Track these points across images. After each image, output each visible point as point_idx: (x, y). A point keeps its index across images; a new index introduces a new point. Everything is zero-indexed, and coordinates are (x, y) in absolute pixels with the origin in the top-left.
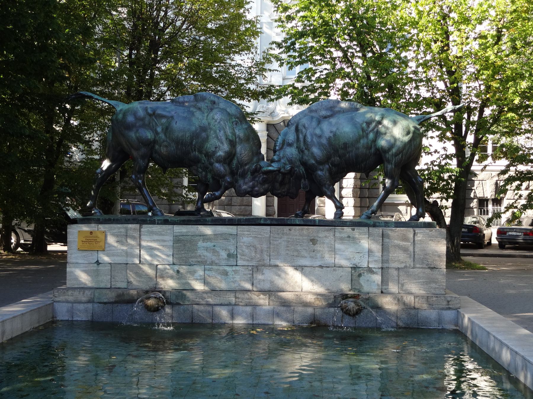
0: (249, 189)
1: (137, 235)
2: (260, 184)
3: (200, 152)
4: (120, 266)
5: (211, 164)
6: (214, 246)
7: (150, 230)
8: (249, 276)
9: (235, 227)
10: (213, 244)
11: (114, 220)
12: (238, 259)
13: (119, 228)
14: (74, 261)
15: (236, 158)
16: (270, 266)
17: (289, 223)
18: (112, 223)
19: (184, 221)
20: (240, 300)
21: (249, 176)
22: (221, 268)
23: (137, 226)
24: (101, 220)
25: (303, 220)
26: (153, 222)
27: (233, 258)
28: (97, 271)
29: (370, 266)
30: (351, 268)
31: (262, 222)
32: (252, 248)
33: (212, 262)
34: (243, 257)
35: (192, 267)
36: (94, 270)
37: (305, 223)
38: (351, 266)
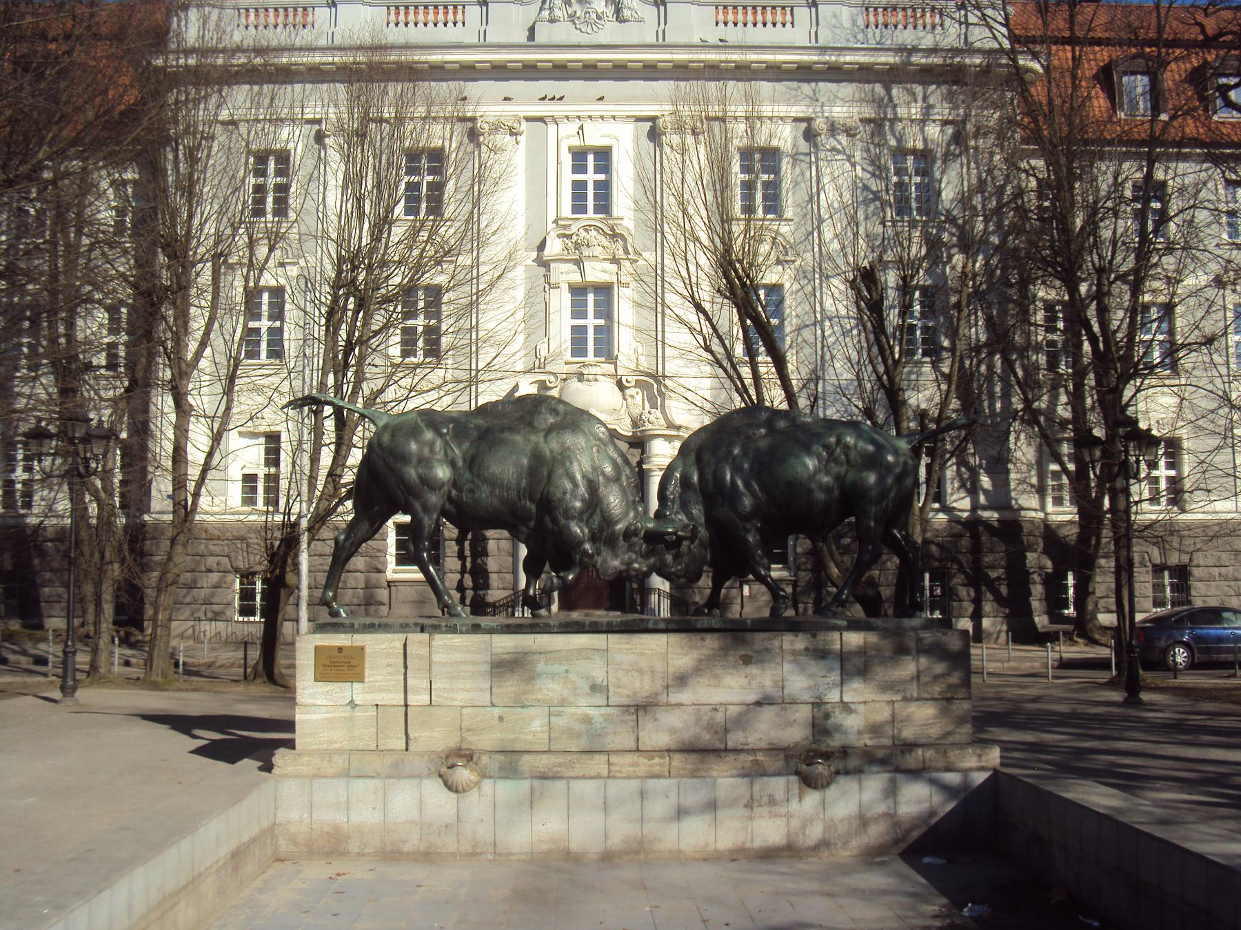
0: (623, 567)
1: (424, 651)
2: (642, 556)
3: (531, 500)
4: (392, 709)
5: (555, 521)
6: (567, 671)
7: (448, 643)
8: (631, 724)
9: (604, 636)
10: (563, 668)
11: (380, 625)
12: (611, 694)
13: (391, 641)
14: (308, 701)
15: (598, 510)
16: (668, 705)
17: (699, 626)
18: (376, 631)
19: (508, 626)
20: (617, 768)
21: (621, 542)
22: (579, 711)
23: (425, 636)
24: (357, 626)
25: (725, 622)
26: (453, 630)
27: (601, 692)
28: (351, 718)
29: (845, 699)
30: (812, 703)
31: (651, 626)
32: (635, 674)
33: (563, 700)
34: (620, 690)
35: (525, 710)
36: (345, 718)
37: (728, 626)
38: (812, 700)
